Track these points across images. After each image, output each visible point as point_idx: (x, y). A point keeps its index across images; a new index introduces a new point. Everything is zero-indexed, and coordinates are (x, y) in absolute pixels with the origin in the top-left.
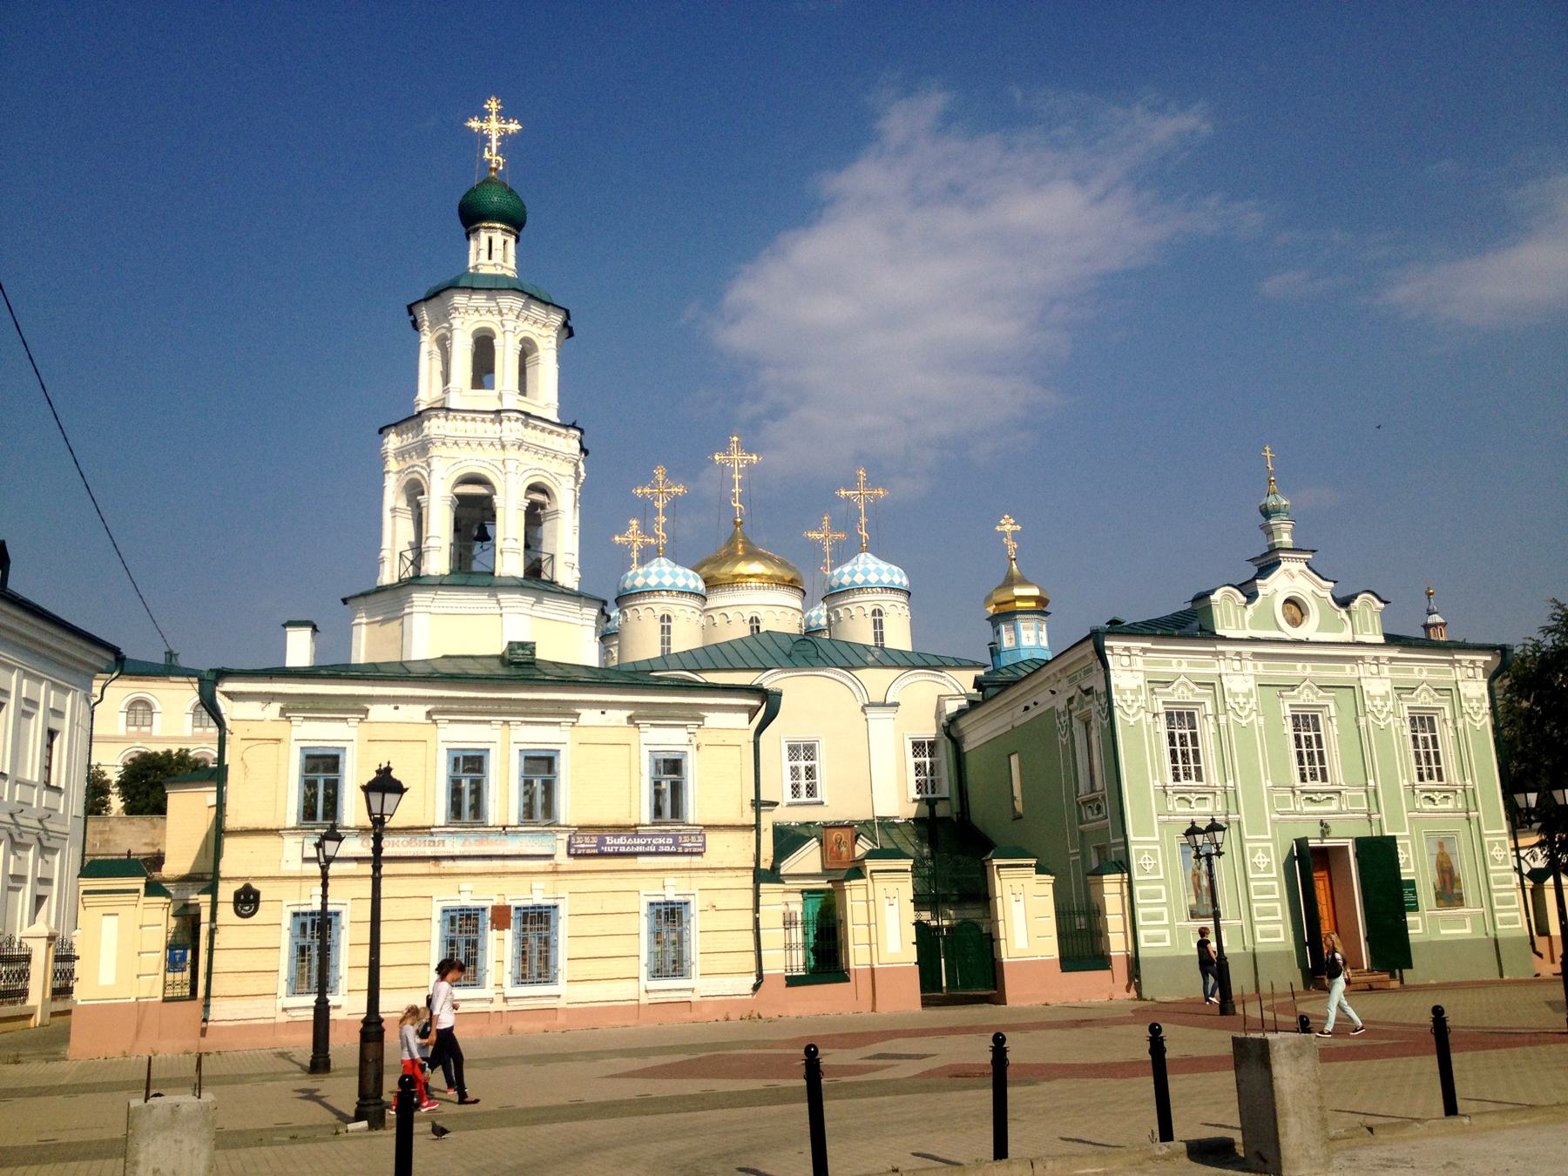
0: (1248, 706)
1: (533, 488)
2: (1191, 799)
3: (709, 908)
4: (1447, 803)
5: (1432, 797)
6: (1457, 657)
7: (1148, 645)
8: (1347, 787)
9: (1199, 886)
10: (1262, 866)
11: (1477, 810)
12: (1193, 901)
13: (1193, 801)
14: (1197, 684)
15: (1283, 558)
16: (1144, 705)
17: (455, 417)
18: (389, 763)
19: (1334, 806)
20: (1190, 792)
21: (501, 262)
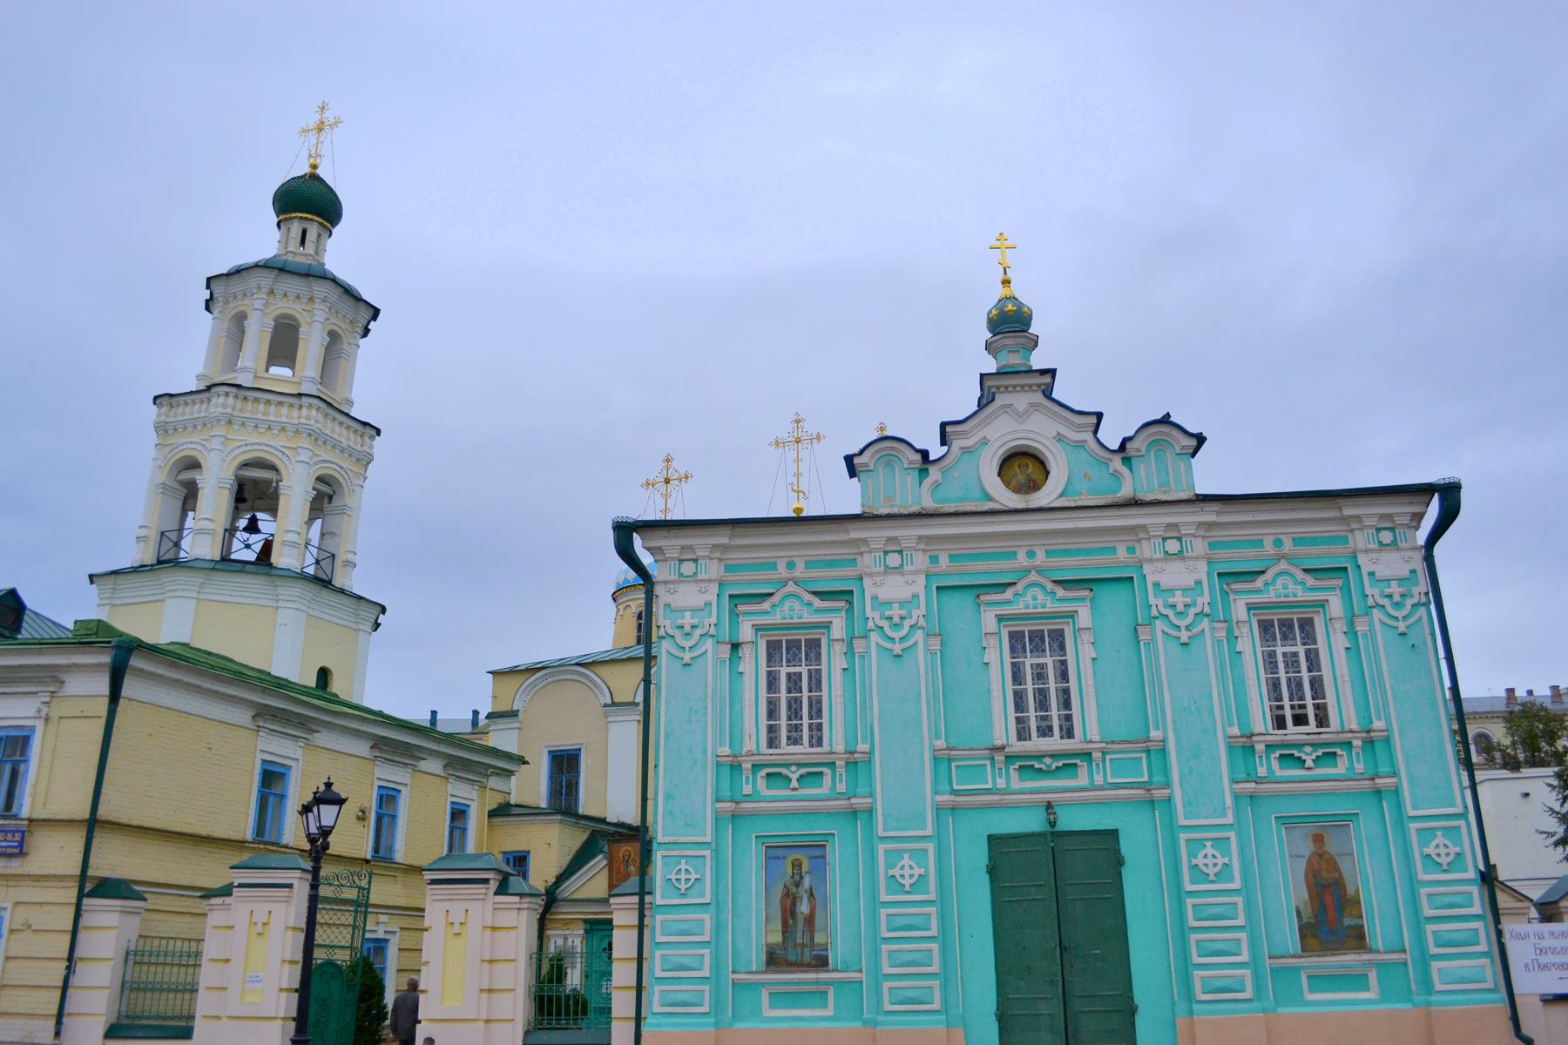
0: (907, 623)
1: (246, 465)
2: (790, 775)
3: (21, 927)
4: (1336, 766)
5: (1297, 754)
6: (1347, 512)
7: (725, 540)
8: (1103, 745)
9: (793, 913)
10: (907, 882)
11: (1394, 775)
12: (777, 938)
13: (794, 777)
14: (815, 593)
15: (998, 387)
16: (713, 631)
17: (178, 402)
18: (329, 778)
19: (1082, 780)
20: (788, 765)
21: (313, 253)
